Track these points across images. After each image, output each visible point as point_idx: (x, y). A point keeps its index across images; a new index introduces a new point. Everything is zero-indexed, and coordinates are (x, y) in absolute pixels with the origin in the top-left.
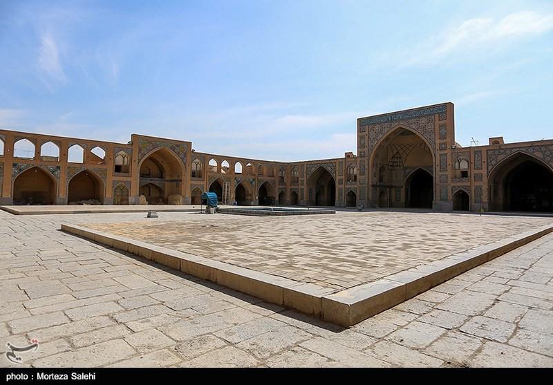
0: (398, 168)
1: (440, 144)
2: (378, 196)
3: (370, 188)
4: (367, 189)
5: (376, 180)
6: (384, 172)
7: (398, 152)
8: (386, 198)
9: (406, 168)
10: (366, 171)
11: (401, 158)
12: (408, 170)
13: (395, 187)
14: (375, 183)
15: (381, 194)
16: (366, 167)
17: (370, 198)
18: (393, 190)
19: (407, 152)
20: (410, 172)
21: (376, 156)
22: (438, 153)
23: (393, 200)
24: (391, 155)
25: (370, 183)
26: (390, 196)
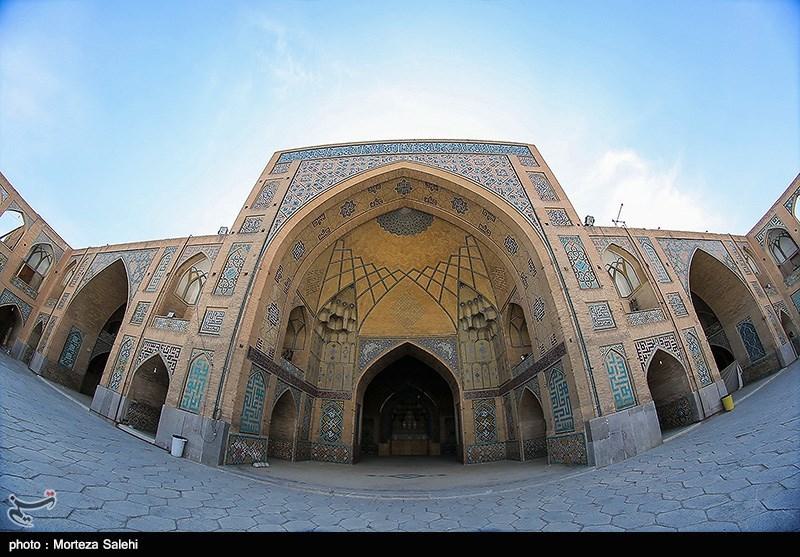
0: (342, 337)
1: (552, 212)
2: (267, 413)
3: (240, 357)
4: (219, 364)
5: (270, 341)
6: (301, 337)
7: (352, 286)
8: (293, 427)
9: (364, 341)
10: (243, 282)
11: (353, 307)
12: (369, 348)
13: (325, 395)
14: (265, 350)
15: (282, 406)
16: (248, 268)
17: (228, 409)
18: (318, 402)
19: (379, 290)
20: (374, 353)
21: (295, 248)
22: (553, 232)
23: (314, 437)
24: (332, 289)
25: (244, 337)
26: (308, 420)
